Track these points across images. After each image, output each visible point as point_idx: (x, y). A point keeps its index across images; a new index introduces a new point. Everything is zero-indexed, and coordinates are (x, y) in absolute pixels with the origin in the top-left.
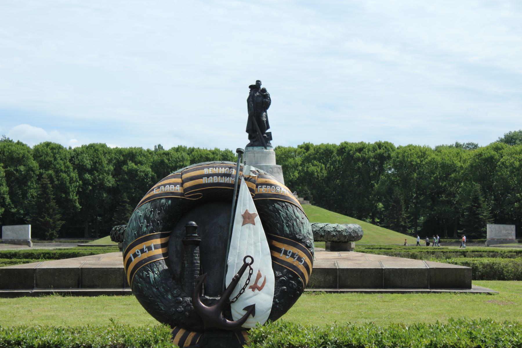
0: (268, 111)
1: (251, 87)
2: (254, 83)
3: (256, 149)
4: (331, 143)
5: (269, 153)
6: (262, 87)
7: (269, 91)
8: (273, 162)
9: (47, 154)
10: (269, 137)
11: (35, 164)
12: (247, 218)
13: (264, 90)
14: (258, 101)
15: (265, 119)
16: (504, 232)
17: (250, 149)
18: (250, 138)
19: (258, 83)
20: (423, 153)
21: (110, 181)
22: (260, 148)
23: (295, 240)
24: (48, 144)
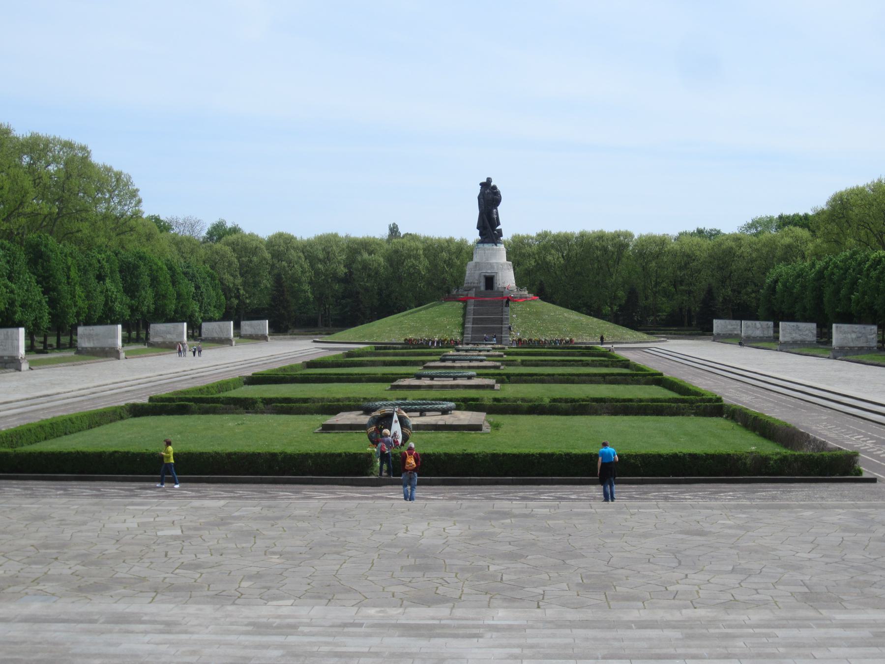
0: (500, 208)
1: (482, 184)
2: (485, 181)
3: (486, 246)
4: (569, 232)
5: (499, 250)
6: (492, 184)
7: (499, 188)
8: (503, 259)
9: (281, 246)
10: (500, 233)
11: (268, 256)
12: (396, 422)
13: (495, 188)
14: (489, 198)
15: (495, 216)
16: (729, 327)
17: (481, 245)
18: (481, 234)
19: (489, 180)
20: (662, 241)
21: (342, 270)
22: (490, 245)
23: (407, 427)
24: (280, 235)
